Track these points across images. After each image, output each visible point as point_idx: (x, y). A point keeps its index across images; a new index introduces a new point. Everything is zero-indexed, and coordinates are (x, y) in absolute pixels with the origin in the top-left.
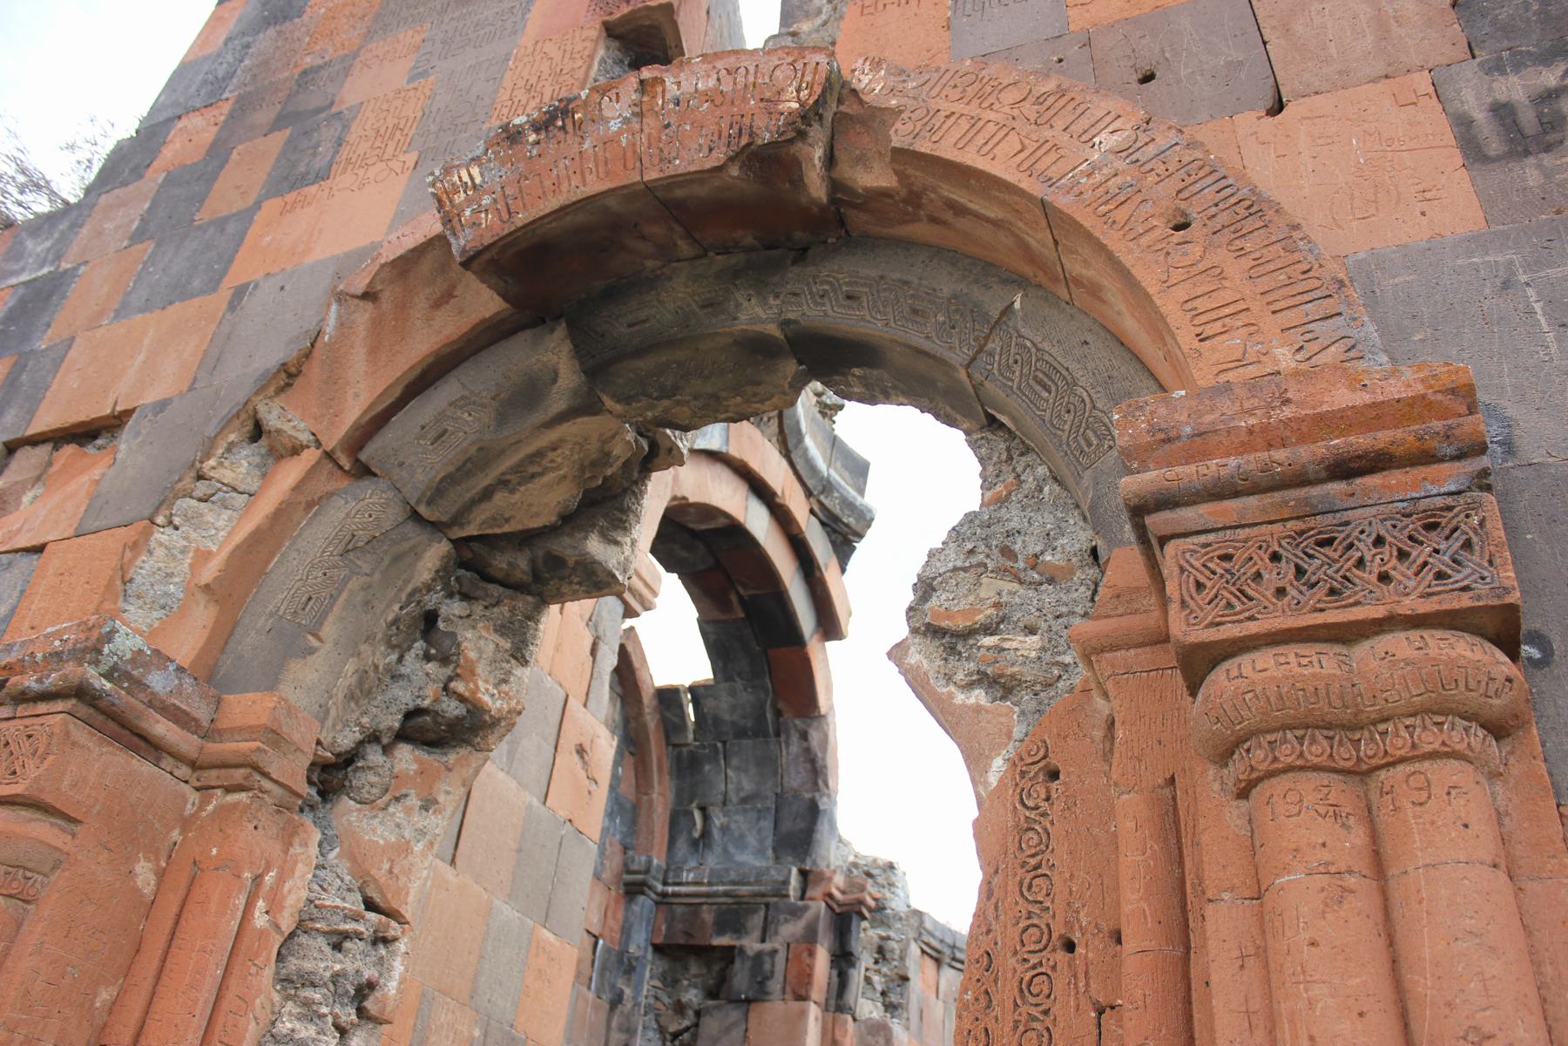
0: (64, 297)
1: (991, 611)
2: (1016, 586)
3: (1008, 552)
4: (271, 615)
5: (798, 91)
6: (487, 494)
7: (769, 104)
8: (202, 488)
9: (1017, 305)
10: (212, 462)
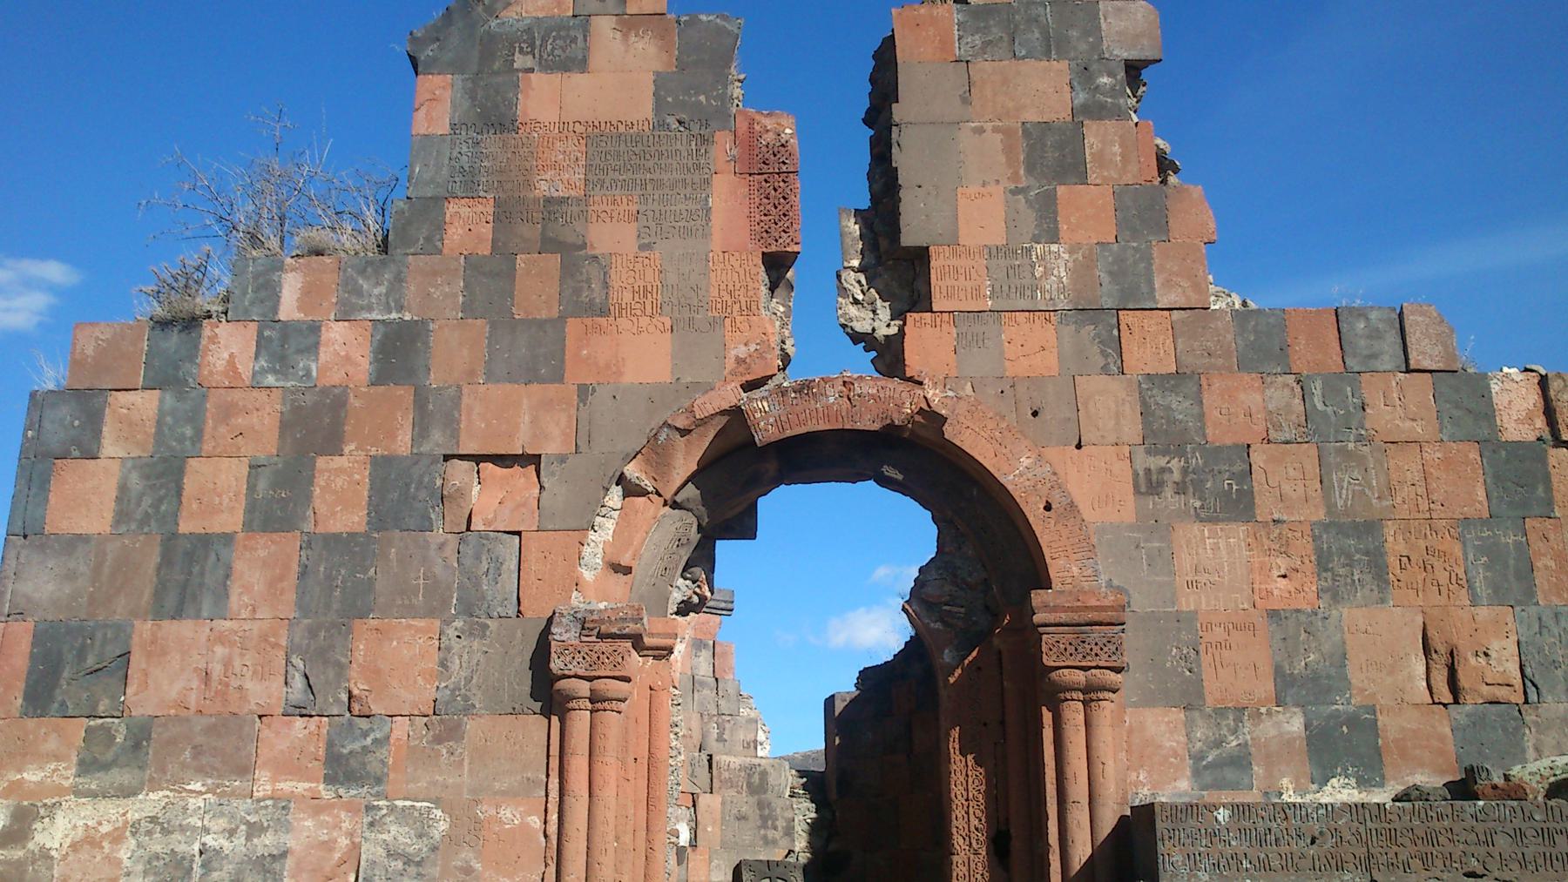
0: (426, 343)
3: (955, 576)
7: (899, 406)
8: (604, 511)
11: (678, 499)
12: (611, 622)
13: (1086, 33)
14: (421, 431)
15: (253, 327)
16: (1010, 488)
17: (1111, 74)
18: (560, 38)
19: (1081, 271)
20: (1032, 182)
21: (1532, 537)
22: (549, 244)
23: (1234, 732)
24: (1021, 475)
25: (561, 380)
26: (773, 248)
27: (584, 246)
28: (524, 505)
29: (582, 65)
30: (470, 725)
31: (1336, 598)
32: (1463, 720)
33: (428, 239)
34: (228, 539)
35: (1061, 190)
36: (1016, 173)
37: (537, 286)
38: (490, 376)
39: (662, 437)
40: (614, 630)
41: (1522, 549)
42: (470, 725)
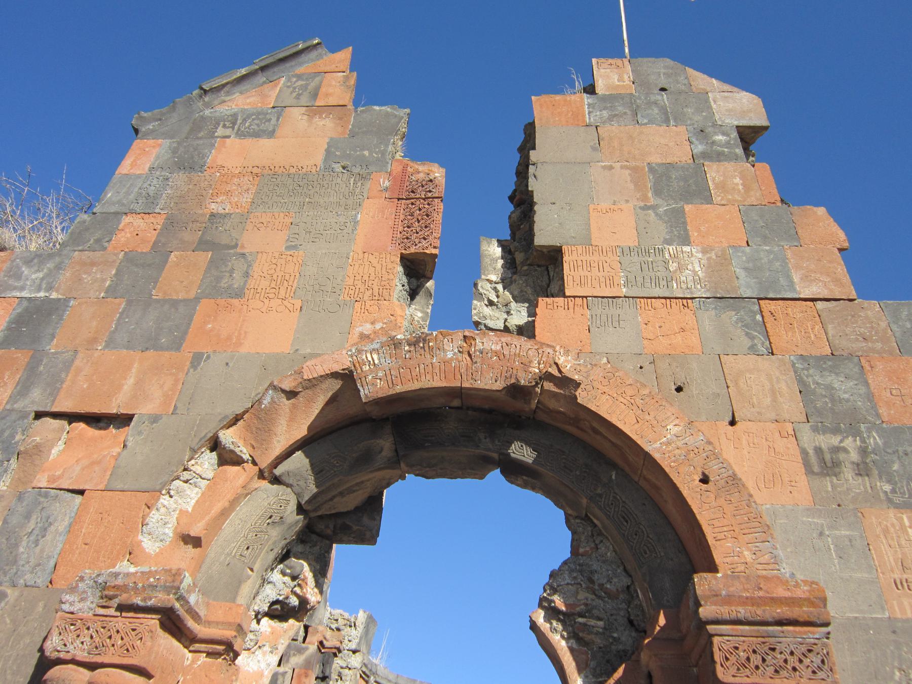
1: (582, 607)
2: (593, 597)
3: (591, 581)
4: (228, 555)
5: (539, 364)
6: (331, 499)
7: (526, 365)
8: (186, 475)
9: (613, 477)
10: (193, 462)
11: (278, 472)
12: (135, 588)
14: (23, 389)
16: (657, 456)
18: (259, 119)
20: (659, 201)
22: (203, 245)
24: (668, 443)
25: (178, 349)
26: (413, 250)
28: (98, 463)
29: (271, 134)
33: (98, 241)
35: (688, 208)
37: (183, 275)
38: (110, 344)
39: (266, 401)
40: (138, 601)
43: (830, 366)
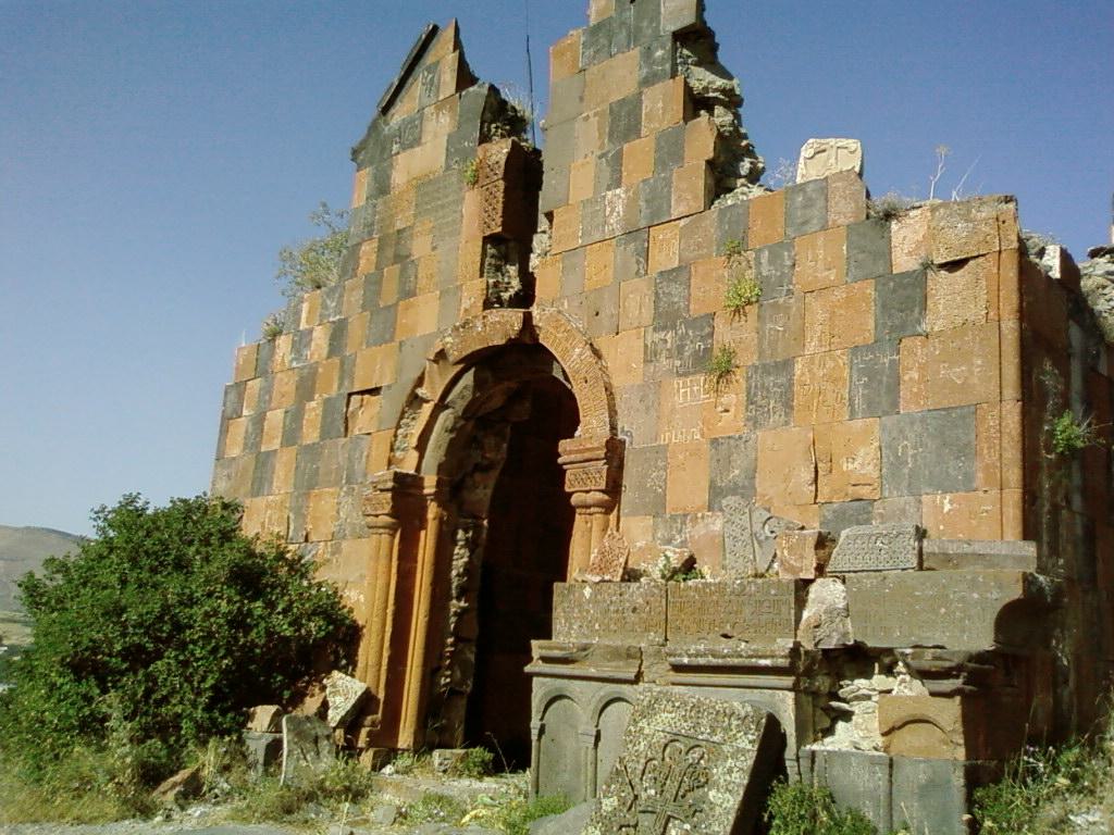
13: (651, 22)
14: (341, 385)
15: (291, 336)
17: (663, 48)
19: (631, 204)
21: (904, 353)
23: (680, 532)
27: (408, 257)
30: (344, 544)
31: (755, 423)
32: (829, 516)
34: (276, 451)
35: (626, 146)
36: (603, 143)
41: (894, 365)
42: (344, 544)
43: (675, 277)
